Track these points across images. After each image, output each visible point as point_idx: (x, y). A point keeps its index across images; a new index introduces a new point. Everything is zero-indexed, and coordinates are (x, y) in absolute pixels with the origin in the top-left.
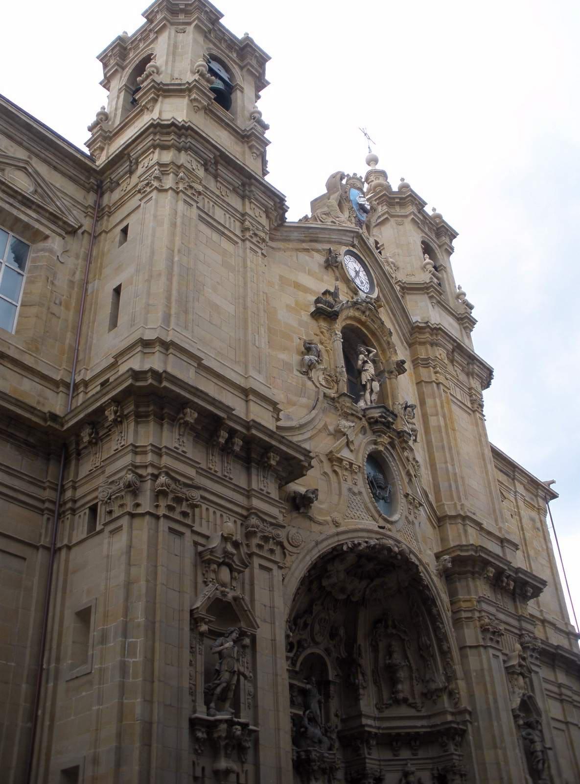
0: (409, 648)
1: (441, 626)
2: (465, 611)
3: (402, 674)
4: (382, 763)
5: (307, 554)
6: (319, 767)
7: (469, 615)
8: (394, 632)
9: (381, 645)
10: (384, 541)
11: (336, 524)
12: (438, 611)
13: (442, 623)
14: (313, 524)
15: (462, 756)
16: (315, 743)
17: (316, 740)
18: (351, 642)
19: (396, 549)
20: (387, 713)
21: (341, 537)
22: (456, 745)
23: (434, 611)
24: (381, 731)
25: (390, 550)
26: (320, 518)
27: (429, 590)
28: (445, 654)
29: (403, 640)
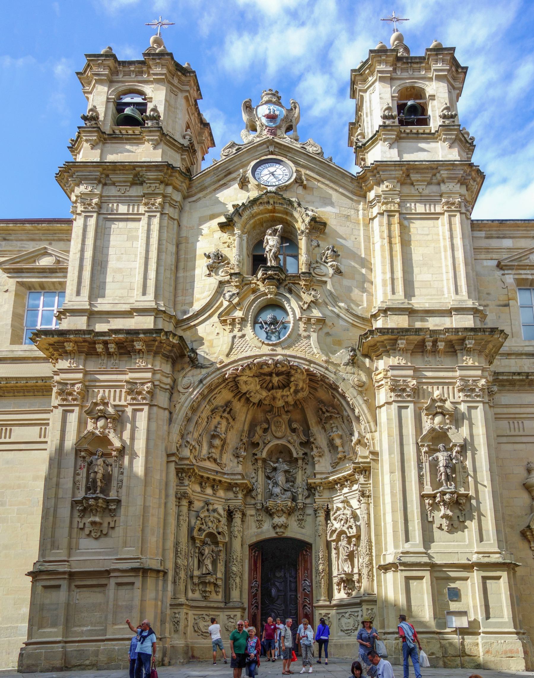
8: (328, 414)
9: (327, 426)
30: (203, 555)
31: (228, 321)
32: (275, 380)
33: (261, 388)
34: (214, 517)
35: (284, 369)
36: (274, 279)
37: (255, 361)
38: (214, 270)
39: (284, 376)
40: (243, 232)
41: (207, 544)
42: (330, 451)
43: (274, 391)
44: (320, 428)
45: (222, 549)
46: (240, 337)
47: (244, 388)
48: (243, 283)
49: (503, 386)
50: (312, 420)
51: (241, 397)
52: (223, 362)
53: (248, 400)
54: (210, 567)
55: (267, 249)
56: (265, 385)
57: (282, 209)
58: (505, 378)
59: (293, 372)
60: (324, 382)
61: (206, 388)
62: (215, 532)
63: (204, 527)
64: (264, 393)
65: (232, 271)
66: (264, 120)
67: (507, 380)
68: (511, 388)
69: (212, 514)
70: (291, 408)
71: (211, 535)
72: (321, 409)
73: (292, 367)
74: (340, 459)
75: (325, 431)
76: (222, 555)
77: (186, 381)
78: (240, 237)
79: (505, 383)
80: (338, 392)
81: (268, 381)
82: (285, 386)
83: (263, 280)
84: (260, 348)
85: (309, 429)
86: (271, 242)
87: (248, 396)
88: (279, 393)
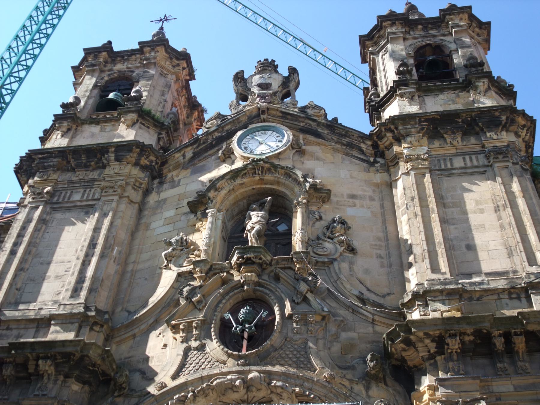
31: (181, 327)
36: (253, 263)
37: (215, 383)
38: (173, 259)
40: (219, 211)
46: (197, 349)
48: (210, 271)
52: (166, 386)
55: (248, 227)
57: (272, 178)
65: (198, 259)
66: (256, 90)
78: (214, 216)
83: (239, 266)
84: (224, 363)
86: (255, 219)
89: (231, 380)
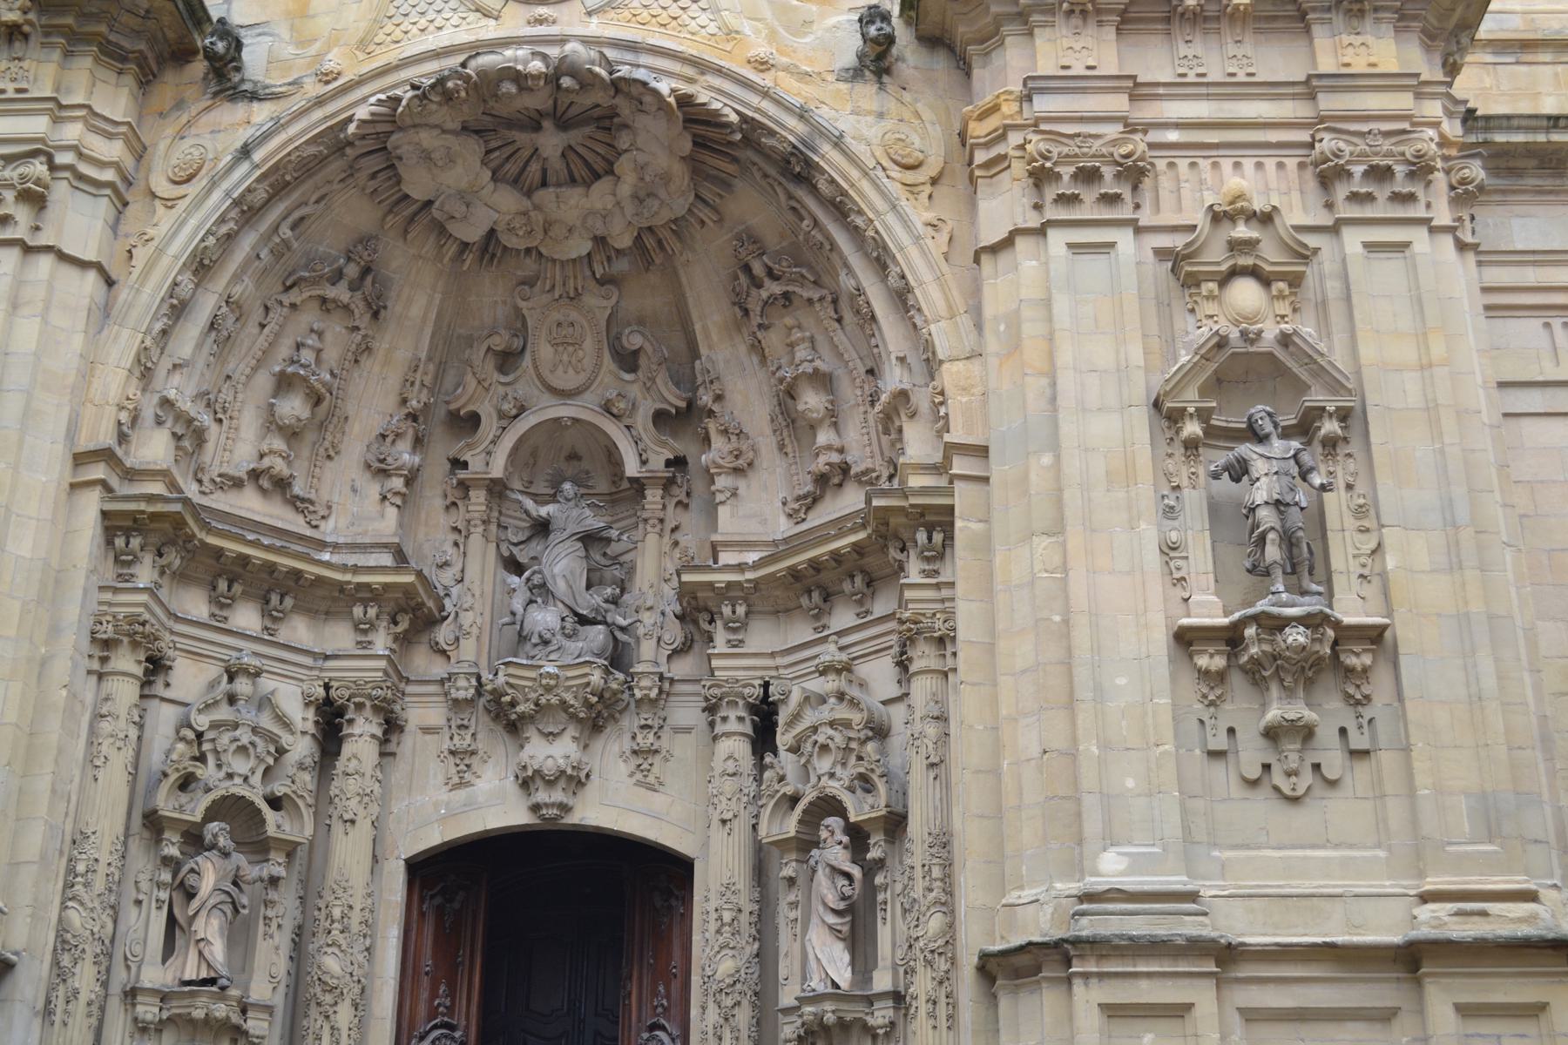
0: (839, 320)
1: (859, 221)
2: (987, 146)
3: (812, 401)
4: (780, 661)
5: (213, 184)
6: (537, 705)
7: (993, 152)
8: (776, 288)
10: (486, 60)
11: (327, 78)
12: (833, 181)
13: (860, 212)
14: (256, 105)
15: (952, 585)
16: (536, 645)
17: (535, 640)
18: (685, 362)
19: (537, 66)
20: (816, 518)
21: (330, 108)
22: (928, 560)
23: (822, 186)
24: (750, 575)
25: (518, 78)
26: (277, 81)
27: (772, 133)
28: (902, 298)
29: (810, 301)
30: (190, 895)
32: (551, 142)
33: (494, 178)
34: (255, 730)
35: (587, 100)
39: (588, 130)
41: (213, 847)
42: (781, 447)
43: (546, 196)
44: (743, 349)
45: (280, 871)
47: (418, 184)
49: (1514, 172)
50: (710, 316)
51: (411, 219)
53: (441, 230)
54: (218, 951)
56: (512, 169)
58: (1519, 138)
59: (625, 108)
60: (759, 149)
61: (264, 176)
62: (255, 794)
63: (208, 772)
64: (507, 201)
67: (1529, 150)
68: (1548, 183)
69: (247, 714)
70: (622, 265)
71: (232, 809)
72: (747, 269)
73: (619, 86)
74: (822, 480)
75: (763, 359)
76: (286, 903)
77: (185, 152)
79: (1520, 163)
80: (814, 190)
81: (526, 153)
82: (591, 171)
85: (694, 354)
87: (435, 213)
88: (571, 205)
89: (516, 60)
